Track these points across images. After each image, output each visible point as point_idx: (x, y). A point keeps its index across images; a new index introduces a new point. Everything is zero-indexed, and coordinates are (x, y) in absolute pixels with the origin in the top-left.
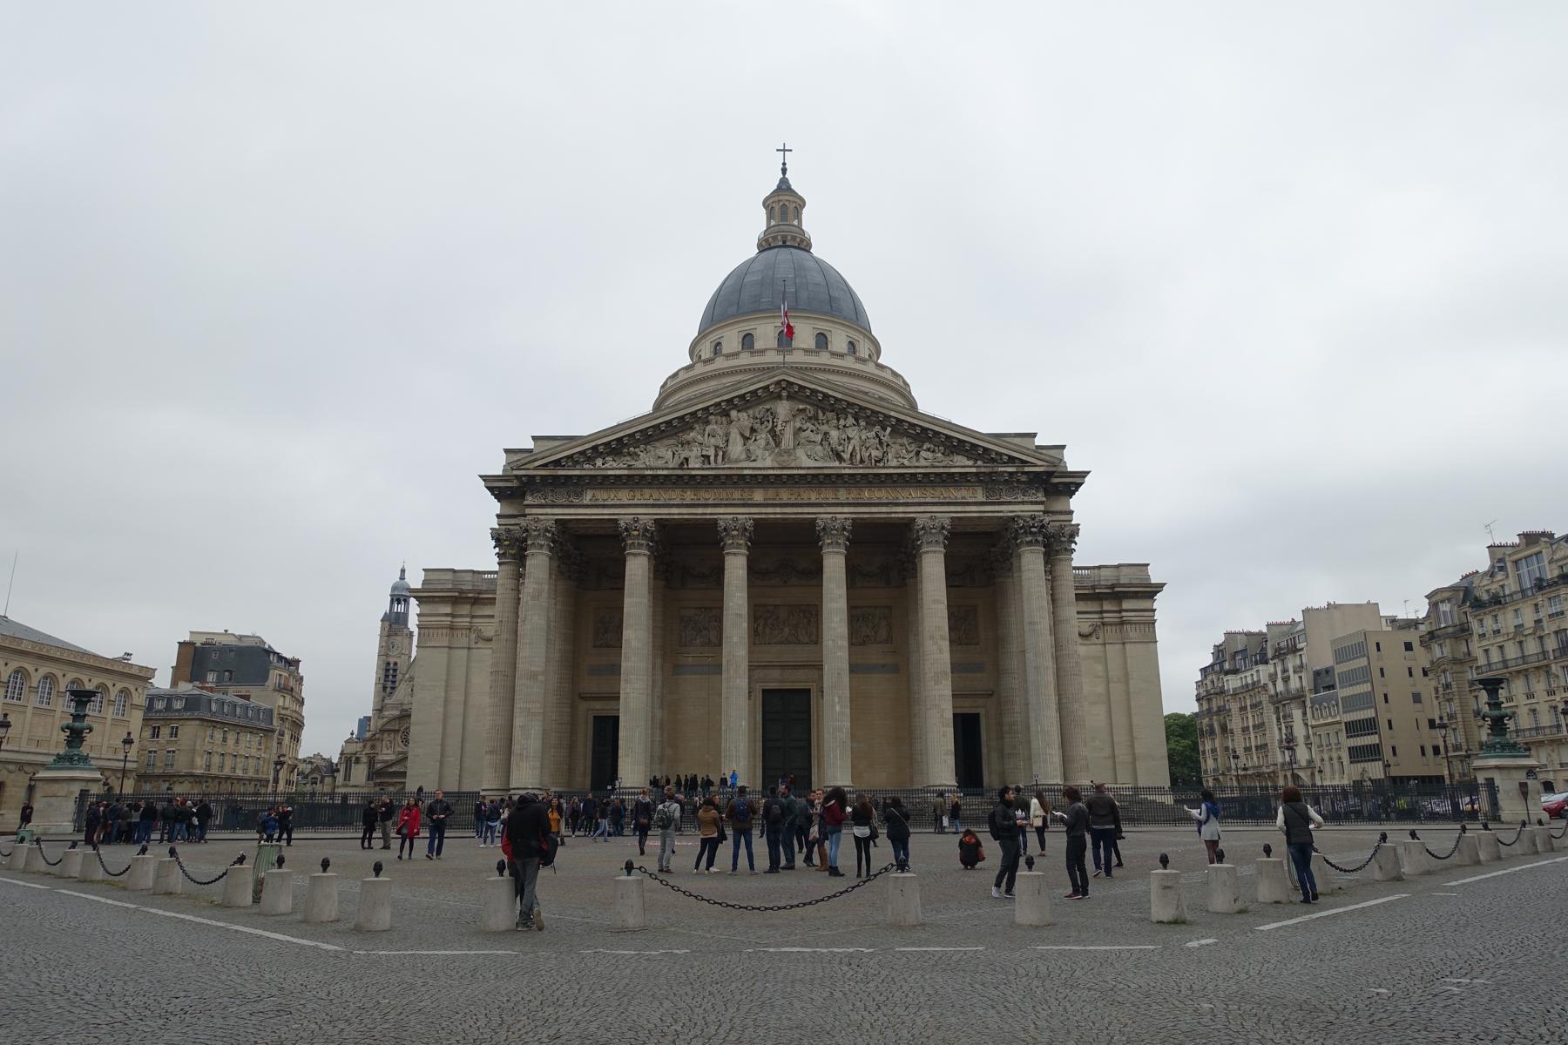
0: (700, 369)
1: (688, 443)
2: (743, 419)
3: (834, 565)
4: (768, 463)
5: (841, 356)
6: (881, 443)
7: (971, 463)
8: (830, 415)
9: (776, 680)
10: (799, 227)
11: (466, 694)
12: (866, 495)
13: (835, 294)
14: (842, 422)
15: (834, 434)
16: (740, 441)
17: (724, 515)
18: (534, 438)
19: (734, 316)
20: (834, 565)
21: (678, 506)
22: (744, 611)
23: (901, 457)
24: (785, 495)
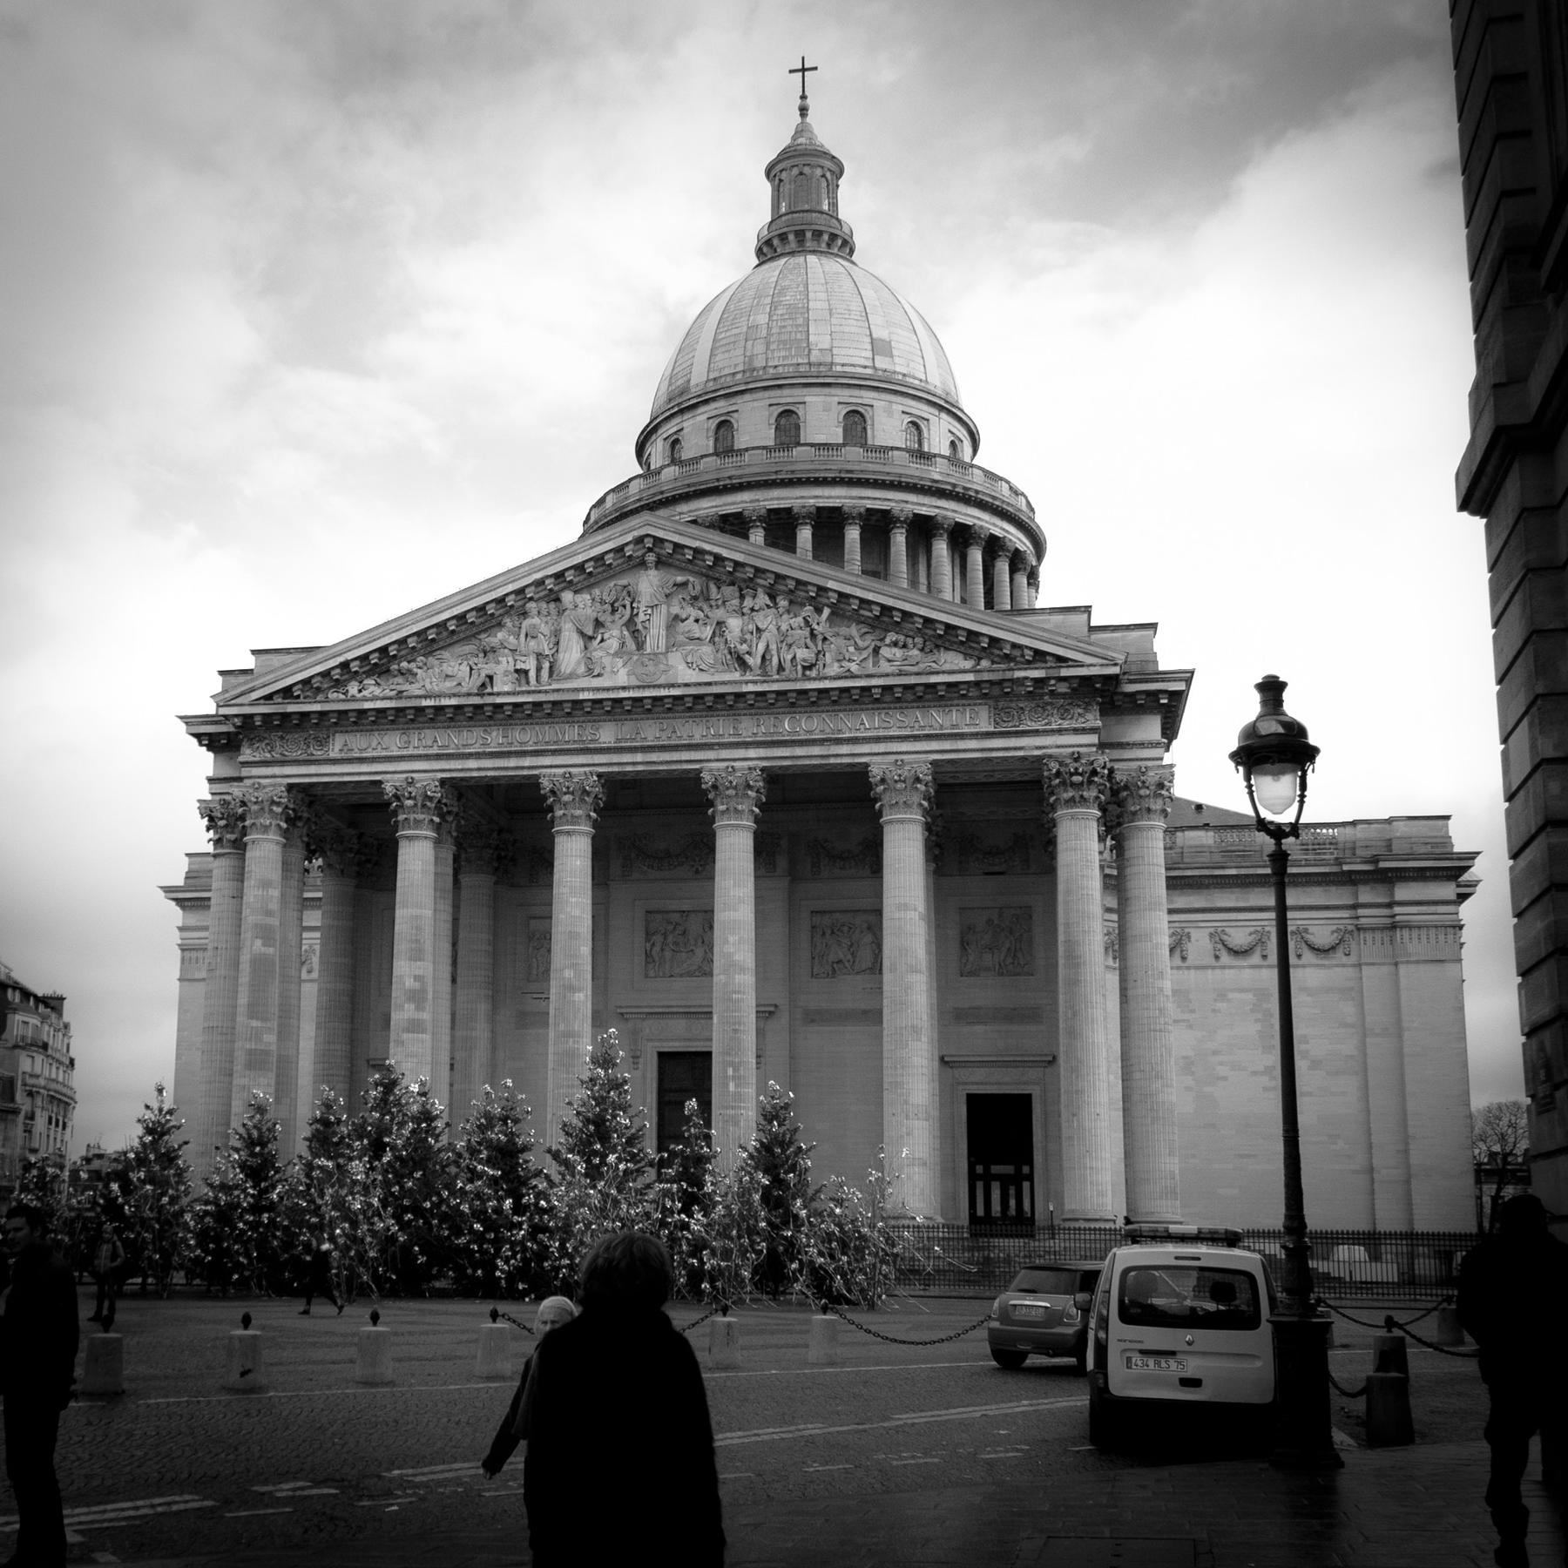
1: (493, 650)
2: (581, 604)
3: (735, 847)
4: (622, 678)
6: (813, 635)
7: (968, 664)
8: (729, 591)
10: (833, 214)
12: (785, 726)
14: (748, 602)
15: (735, 624)
17: (550, 769)
18: (254, 652)
20: (735, 847)
21: (478, 756)
23: (848, 659)
24: (651, 731)
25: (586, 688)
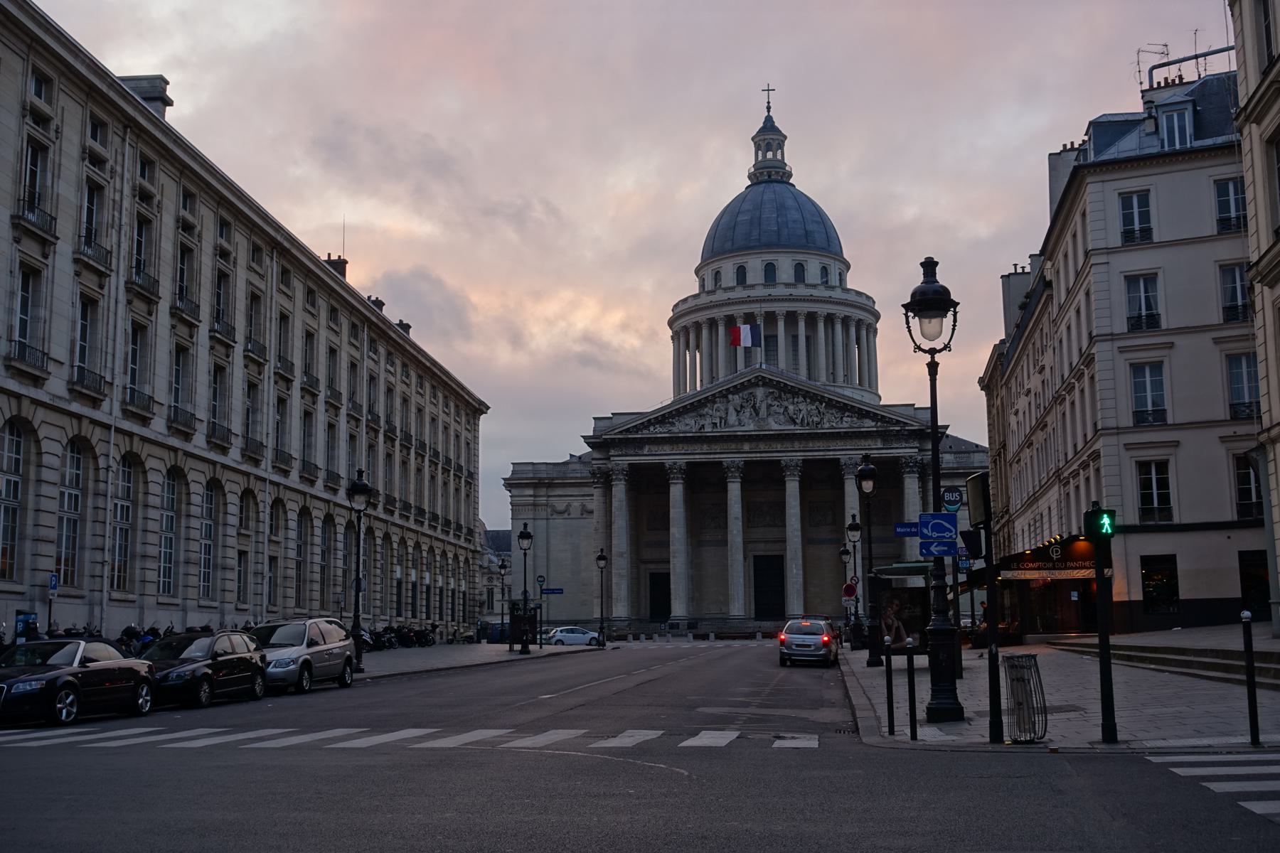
0: (705, 299)
2: (736, 399)
3: (793, 487)
4: (752, 427)
5: (814, 286)
9: (761, 549)
11: (548, 551)
13: (810, 227)
15: (791, 408)
16: (734, 414)
17: (726, 458)
19: (731, 251)
20: (793, 487)
22: (740, 516)
23: (832, 422)
24: (762, 447)
25: (740, 431)
